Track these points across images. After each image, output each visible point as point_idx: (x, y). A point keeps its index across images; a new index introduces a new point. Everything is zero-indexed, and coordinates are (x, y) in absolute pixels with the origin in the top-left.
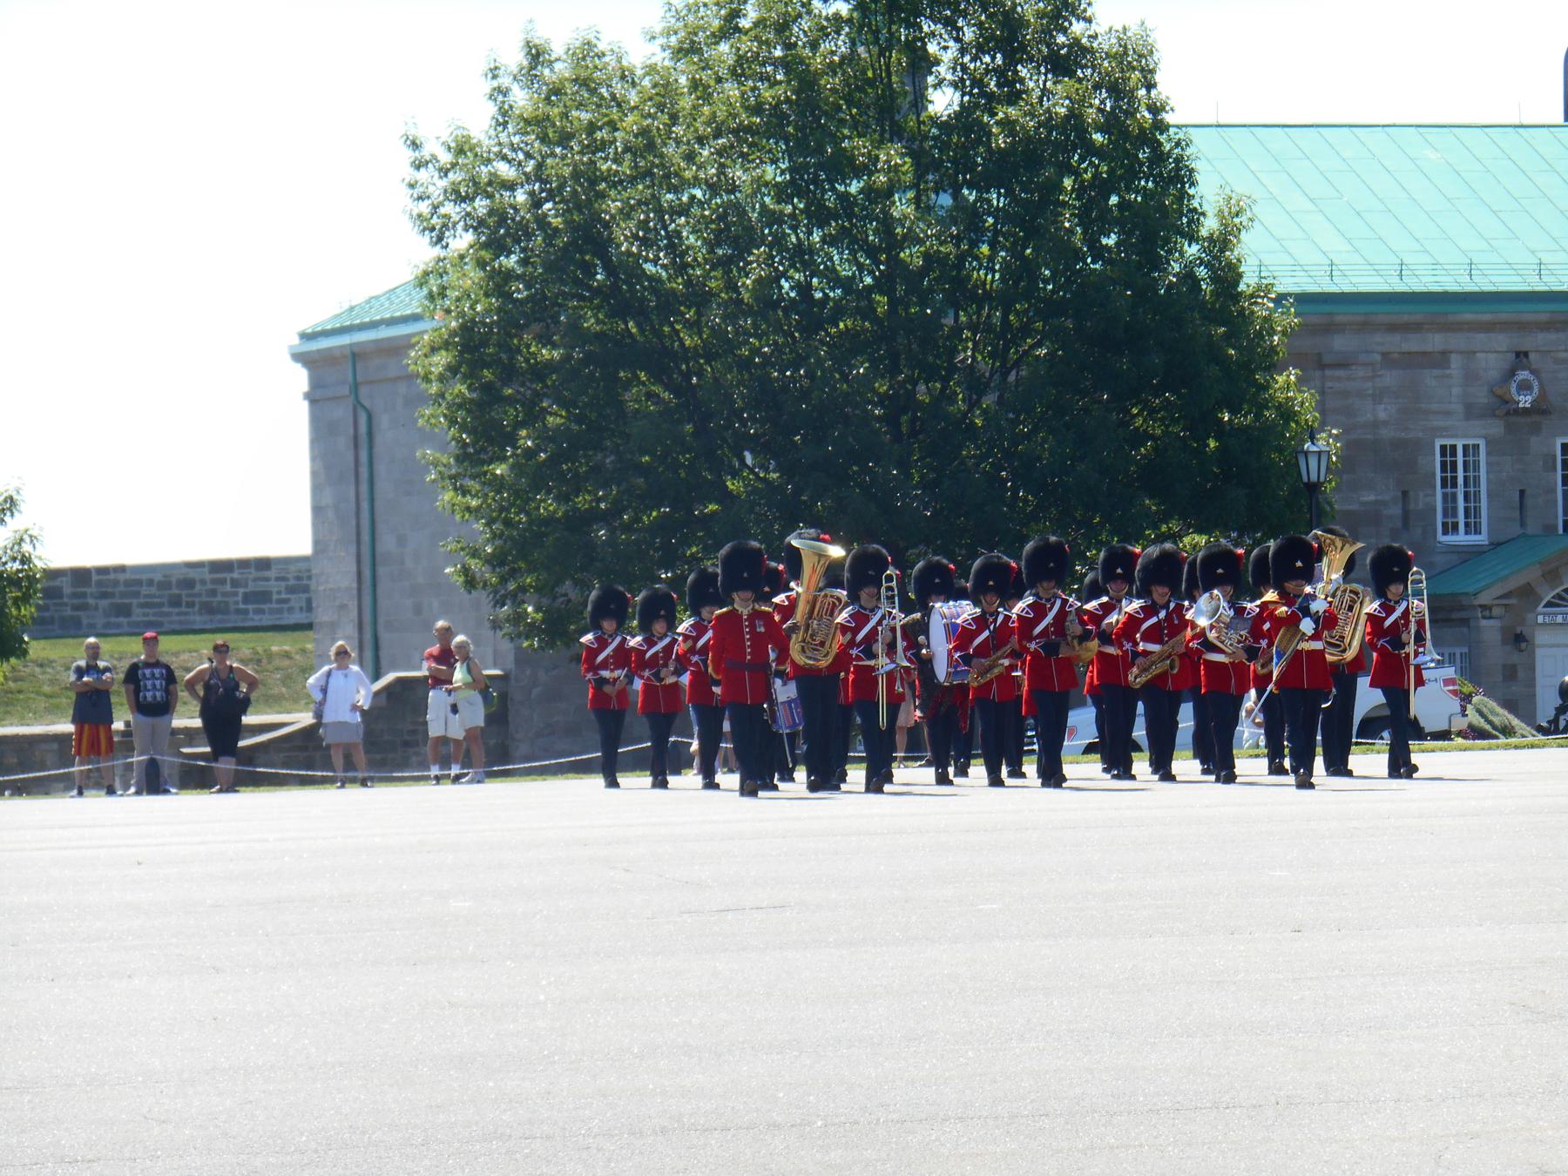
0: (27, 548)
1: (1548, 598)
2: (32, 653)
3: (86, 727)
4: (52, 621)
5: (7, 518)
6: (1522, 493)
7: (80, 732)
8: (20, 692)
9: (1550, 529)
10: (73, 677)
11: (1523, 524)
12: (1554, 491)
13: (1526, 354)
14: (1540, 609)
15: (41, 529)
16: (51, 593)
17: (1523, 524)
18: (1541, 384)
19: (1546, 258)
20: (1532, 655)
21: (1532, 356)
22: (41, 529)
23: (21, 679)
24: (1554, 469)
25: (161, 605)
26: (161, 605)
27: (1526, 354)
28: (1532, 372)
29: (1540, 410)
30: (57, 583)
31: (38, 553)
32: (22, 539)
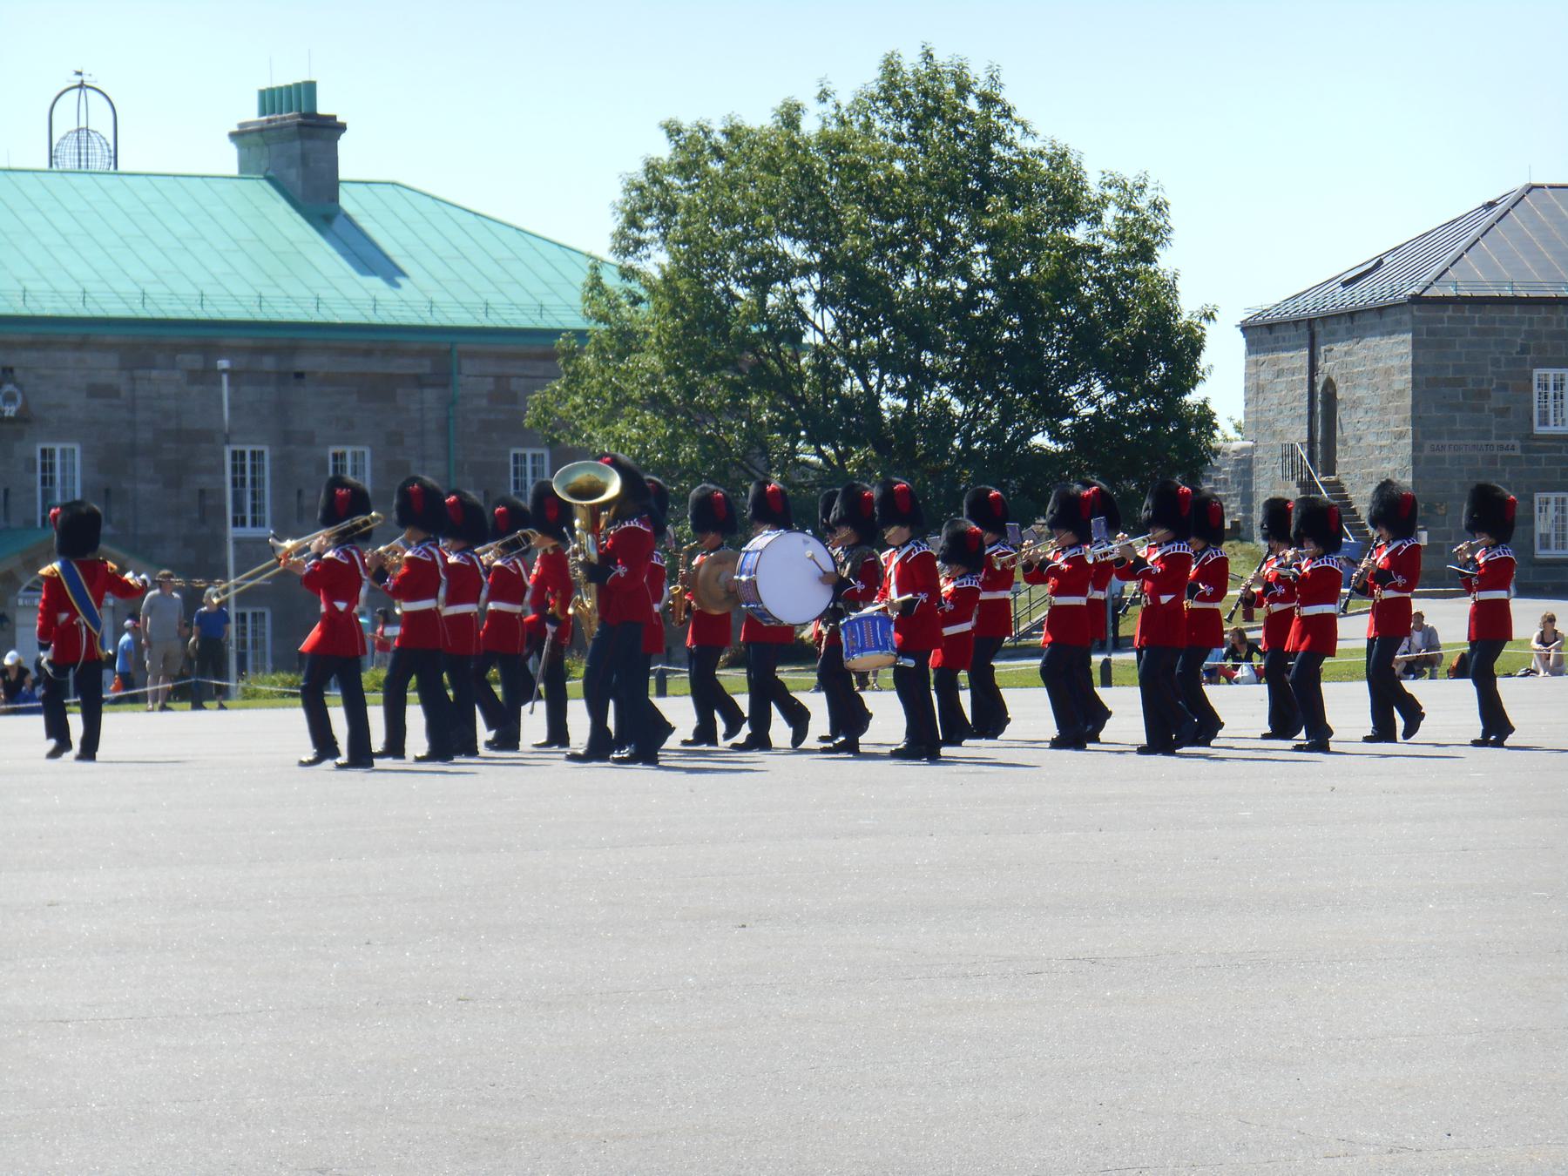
1: (26, 585)
6: (6, 492)
9: (30, 524)
11: (7, 517)
12: (33, 490)
13: (11, 370)
14: (21, 592)
17: (7, 517)
18: (25, 398)
19: (30, 286)
20: (13, 631)
21: (17, 372)
24: (34, 470)
27: (11, 370)
28: (17, 385)
29: (23, 418)
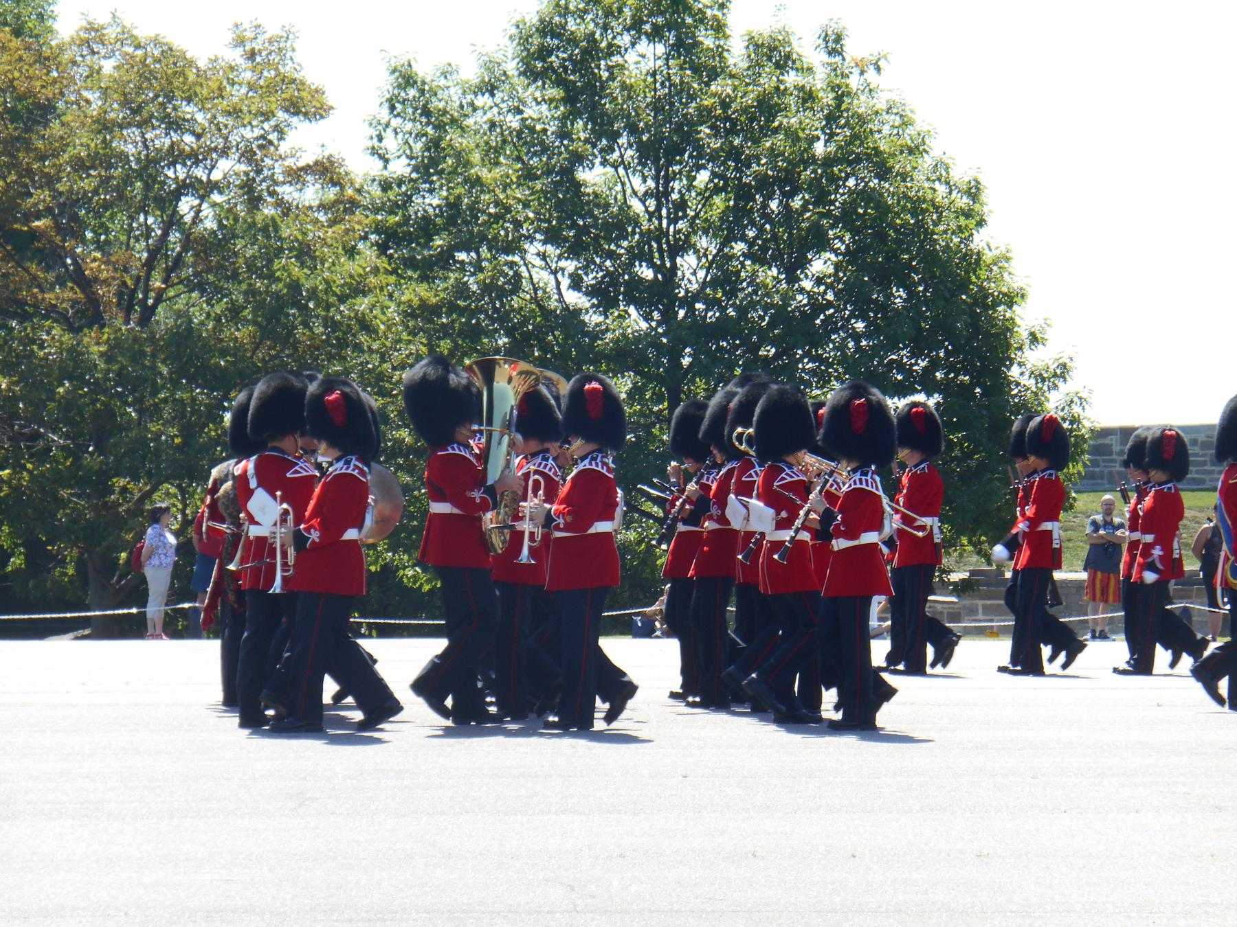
0: (1076, 409)
2: (1079, 505)
3: (1099, 574)
4: (1101, 476)
5: (1060, 384)
7: (1092, 579)
8: (1069, 540)
10: (1089, 530)
15: (1090, 392)
16: (1098, 450)
22: (1090, 392)
23: (1071, 529)
25: (1204, 463)
26: (1204, 463)
30: (1107, 441)
31: (1085, 414)
32: (1072, 402)
